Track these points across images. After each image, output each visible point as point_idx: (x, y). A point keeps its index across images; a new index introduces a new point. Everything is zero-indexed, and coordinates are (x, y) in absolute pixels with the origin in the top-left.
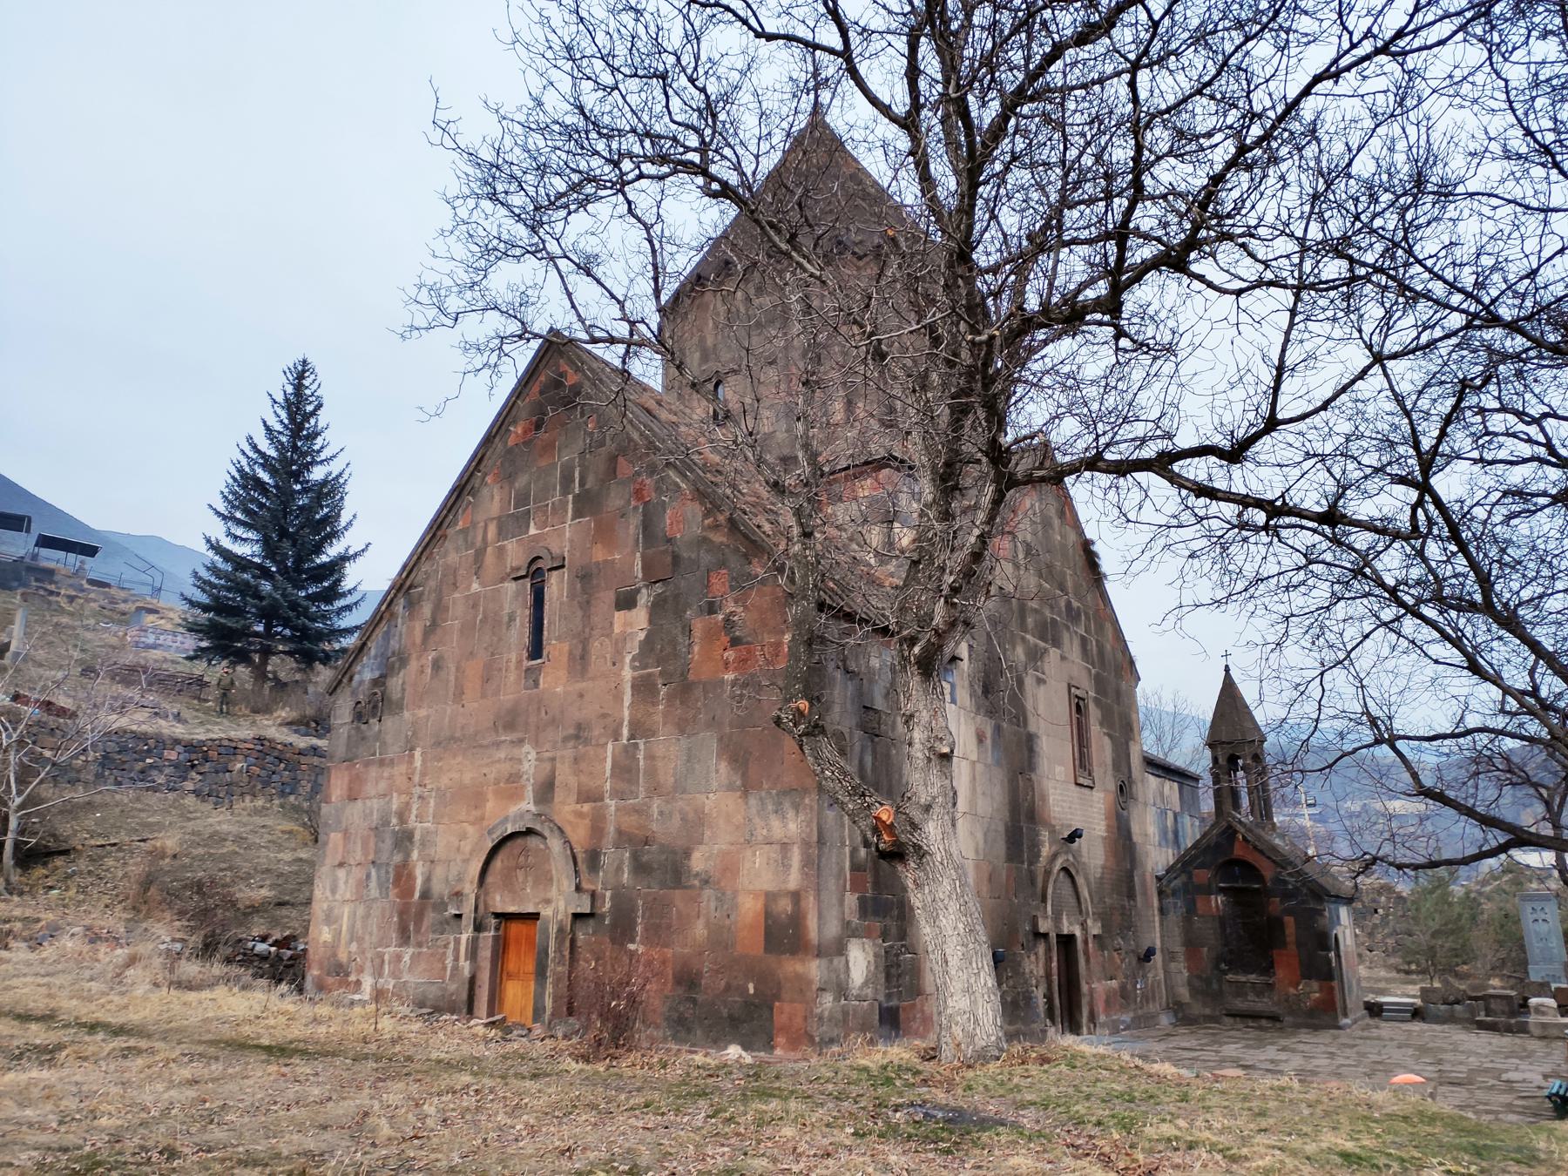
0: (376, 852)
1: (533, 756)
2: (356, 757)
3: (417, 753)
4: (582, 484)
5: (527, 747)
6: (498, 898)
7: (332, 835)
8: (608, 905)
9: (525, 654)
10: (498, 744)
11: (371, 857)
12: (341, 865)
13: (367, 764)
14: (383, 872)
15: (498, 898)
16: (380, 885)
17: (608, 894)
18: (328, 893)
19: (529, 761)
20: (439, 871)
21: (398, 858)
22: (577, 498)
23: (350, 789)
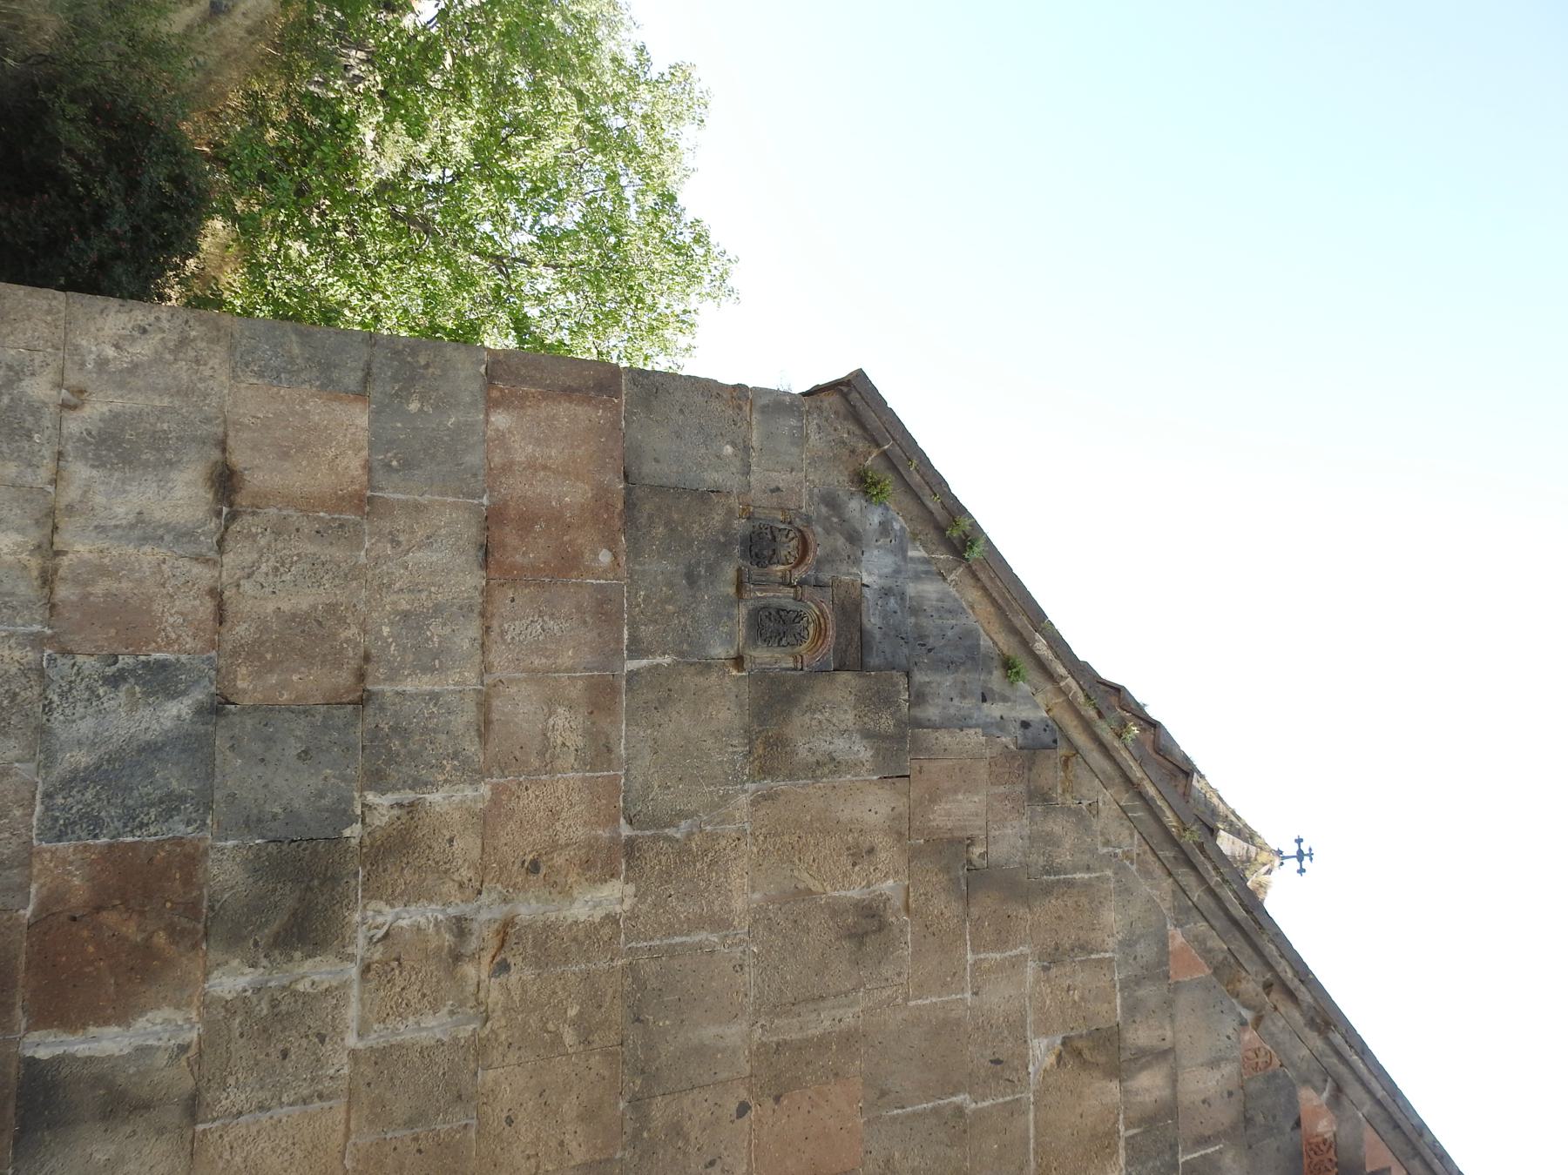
0: (266, 711)
2: (635, 552)
3: (614, 895)
7: (360, 417)
11: (243, 681)
12: (225, 482)
13: (604, 610)
14: (172, 777)
16: (114, 770)
18: (96, 410)
21: (226, 868)
23: (526, 522)
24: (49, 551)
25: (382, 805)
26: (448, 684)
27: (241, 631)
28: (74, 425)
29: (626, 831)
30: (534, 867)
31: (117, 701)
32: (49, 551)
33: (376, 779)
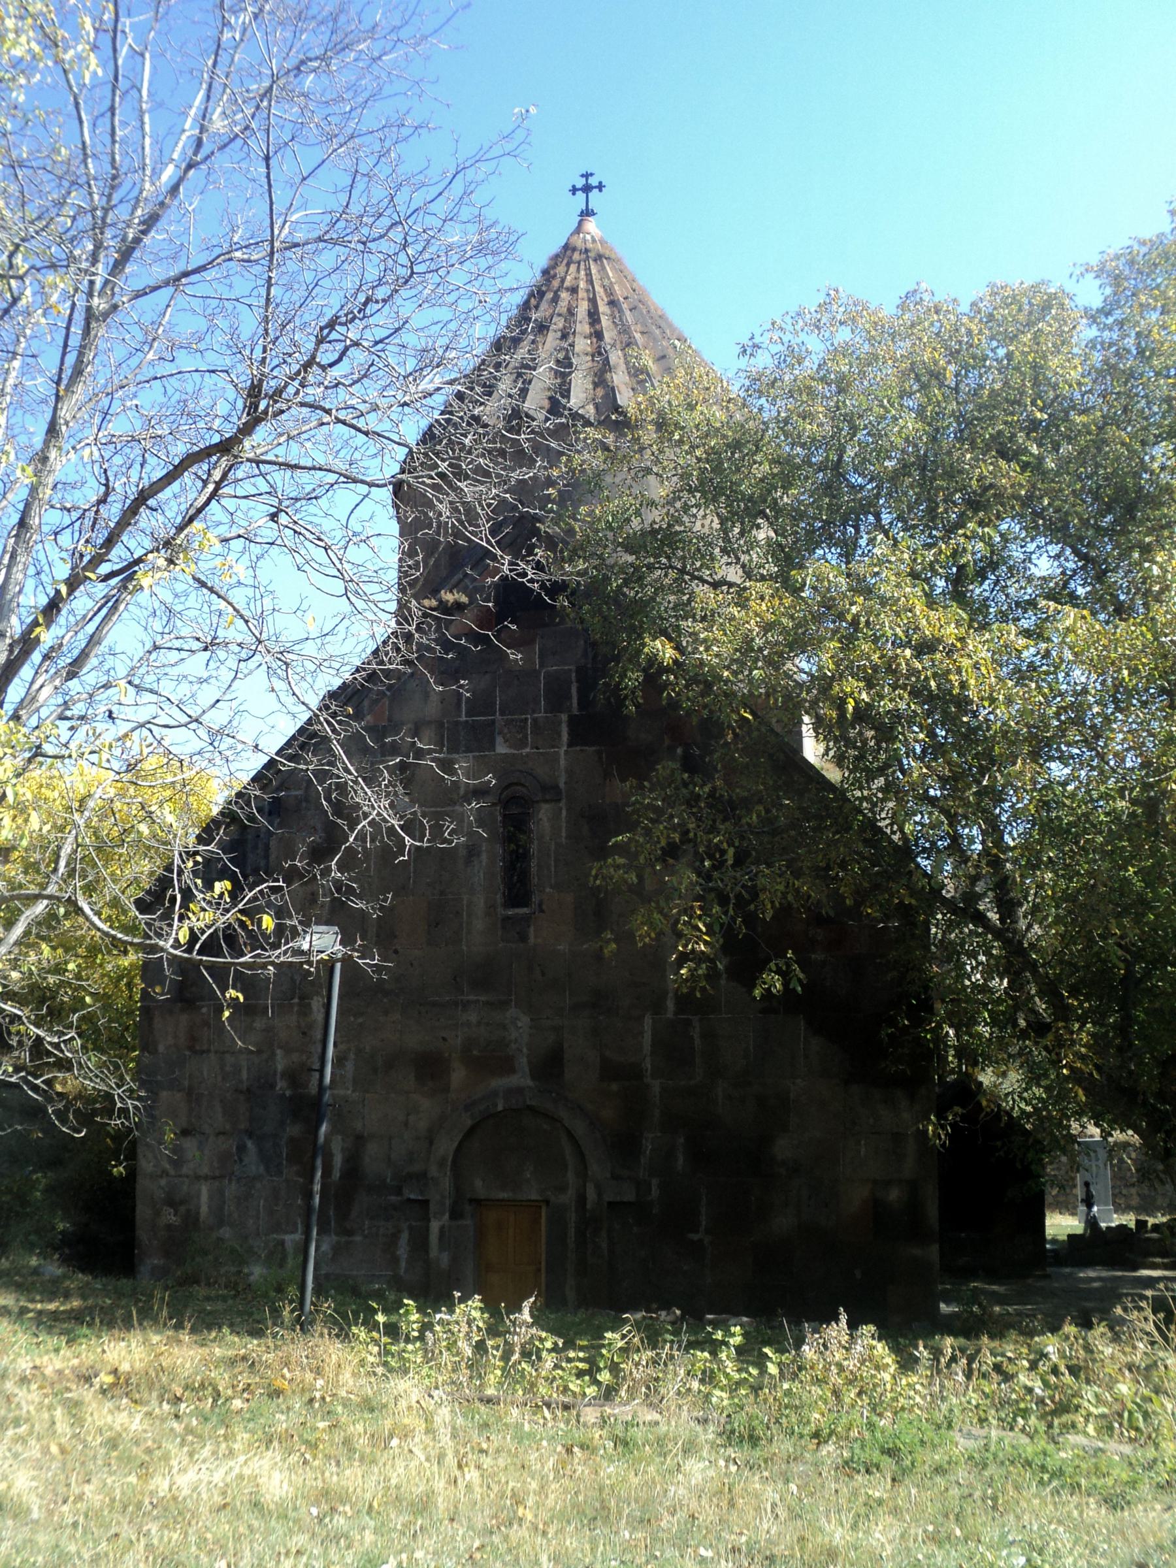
1: (524, 1021)
4: (584, 703)
5: (512, 1012)
6: (478, 1183)
8: (655, 1192)
9: (499, 898)
10: (466, 1005)
11: (242, 1127)
15: (478, 1183)
17: (655, 1182)
19: (519, 1028)
20: (372, 1149)
22: (573, 722)
24: (206, 1178)
25: (281, 1085)
26: (244, 1063)
27: (228, 1127)
28: (172, 1172)
29: (296, 1000)
30: (304, 1033)
31: (246, 1160)
32: (206, 1178)
33: (272, 1086)
